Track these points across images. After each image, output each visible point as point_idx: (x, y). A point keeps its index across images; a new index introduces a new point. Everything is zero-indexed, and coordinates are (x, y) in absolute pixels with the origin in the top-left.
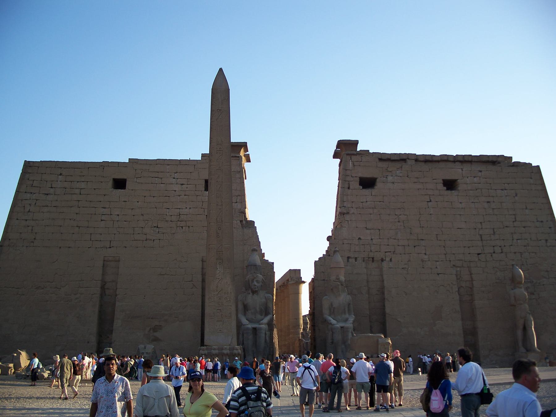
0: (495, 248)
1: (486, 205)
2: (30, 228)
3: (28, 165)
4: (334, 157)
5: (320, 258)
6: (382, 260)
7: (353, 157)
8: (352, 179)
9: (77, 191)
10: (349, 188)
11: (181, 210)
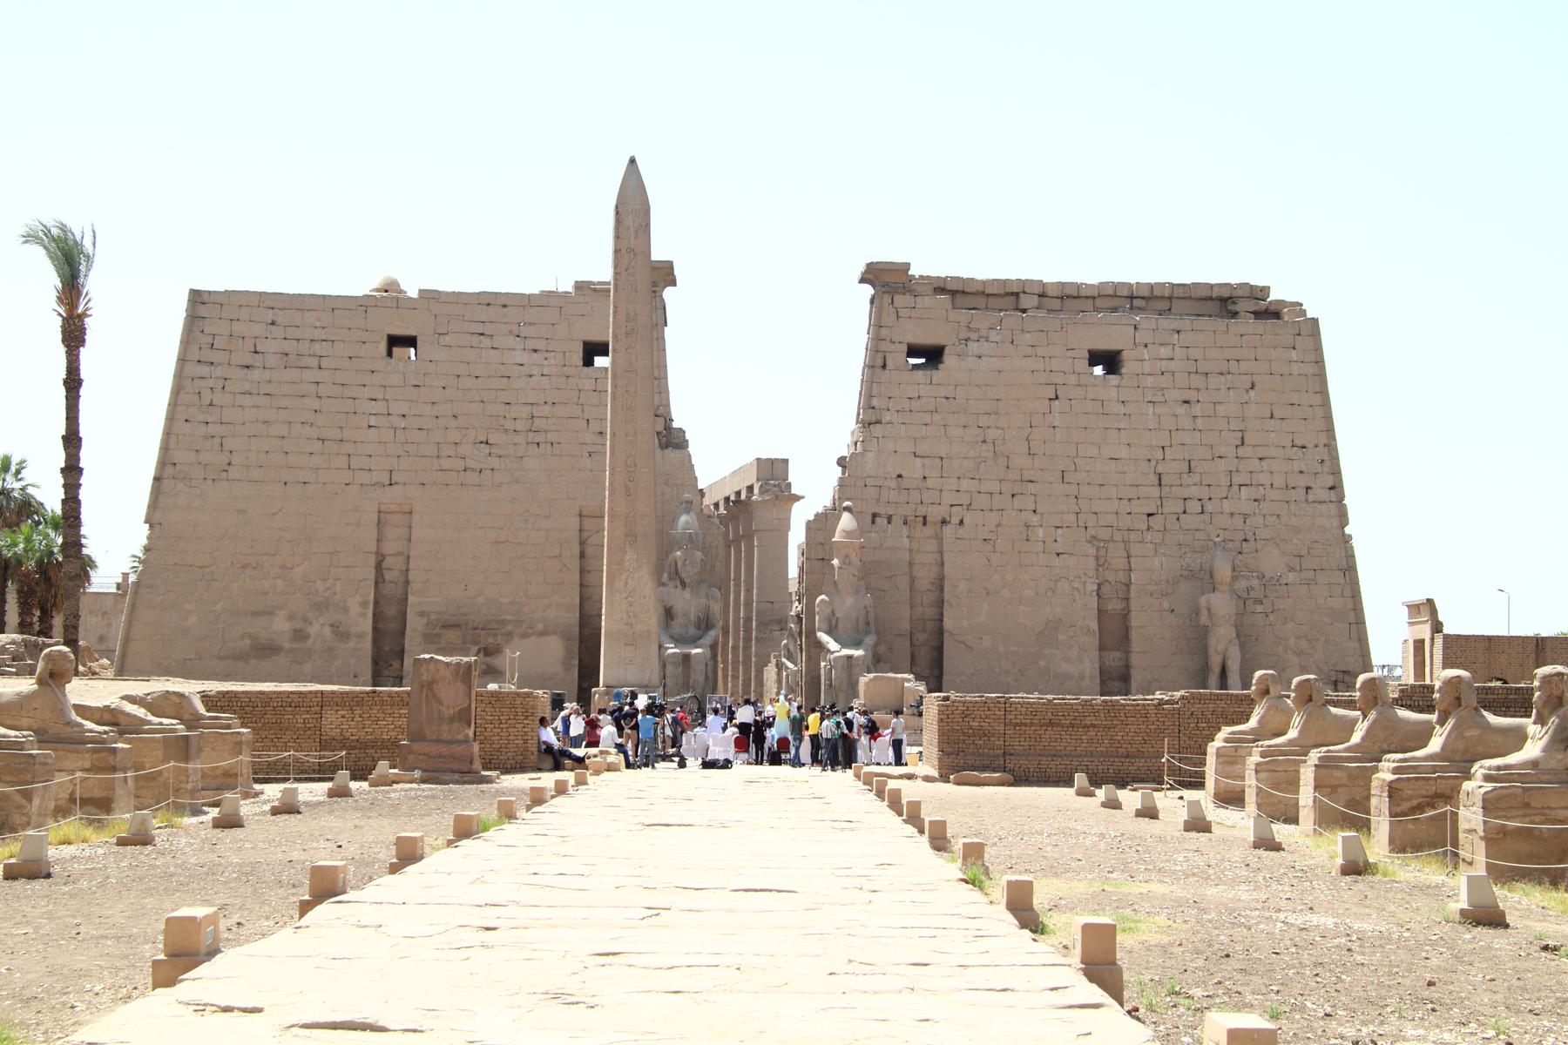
0: (1188, 503)
1: (1182, 410)
2: (217, 441)
3: (196, 298)
4: (862, 281)
5: (817, 515)
6: (944, 522)
7: (897, 298)
8: (893, 347)
9: (313, 362)
10: (884, 367)
11: (535, 408)
